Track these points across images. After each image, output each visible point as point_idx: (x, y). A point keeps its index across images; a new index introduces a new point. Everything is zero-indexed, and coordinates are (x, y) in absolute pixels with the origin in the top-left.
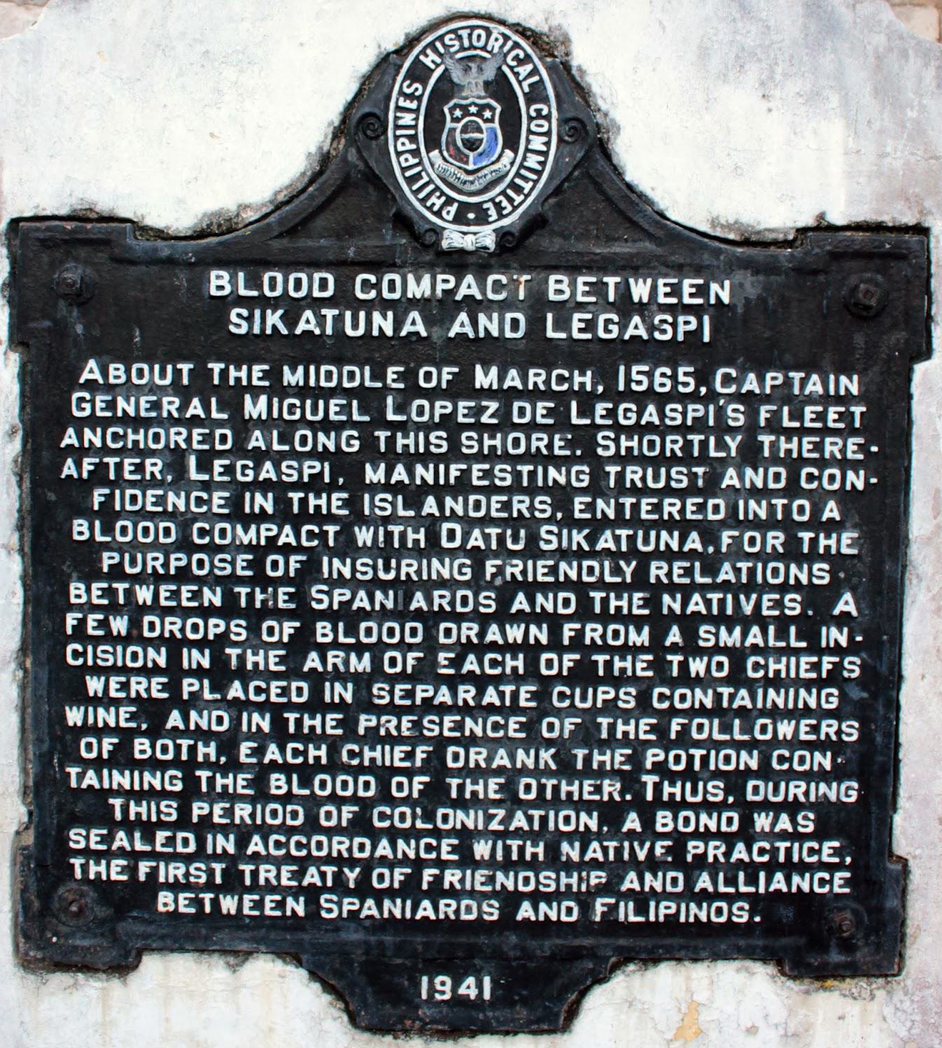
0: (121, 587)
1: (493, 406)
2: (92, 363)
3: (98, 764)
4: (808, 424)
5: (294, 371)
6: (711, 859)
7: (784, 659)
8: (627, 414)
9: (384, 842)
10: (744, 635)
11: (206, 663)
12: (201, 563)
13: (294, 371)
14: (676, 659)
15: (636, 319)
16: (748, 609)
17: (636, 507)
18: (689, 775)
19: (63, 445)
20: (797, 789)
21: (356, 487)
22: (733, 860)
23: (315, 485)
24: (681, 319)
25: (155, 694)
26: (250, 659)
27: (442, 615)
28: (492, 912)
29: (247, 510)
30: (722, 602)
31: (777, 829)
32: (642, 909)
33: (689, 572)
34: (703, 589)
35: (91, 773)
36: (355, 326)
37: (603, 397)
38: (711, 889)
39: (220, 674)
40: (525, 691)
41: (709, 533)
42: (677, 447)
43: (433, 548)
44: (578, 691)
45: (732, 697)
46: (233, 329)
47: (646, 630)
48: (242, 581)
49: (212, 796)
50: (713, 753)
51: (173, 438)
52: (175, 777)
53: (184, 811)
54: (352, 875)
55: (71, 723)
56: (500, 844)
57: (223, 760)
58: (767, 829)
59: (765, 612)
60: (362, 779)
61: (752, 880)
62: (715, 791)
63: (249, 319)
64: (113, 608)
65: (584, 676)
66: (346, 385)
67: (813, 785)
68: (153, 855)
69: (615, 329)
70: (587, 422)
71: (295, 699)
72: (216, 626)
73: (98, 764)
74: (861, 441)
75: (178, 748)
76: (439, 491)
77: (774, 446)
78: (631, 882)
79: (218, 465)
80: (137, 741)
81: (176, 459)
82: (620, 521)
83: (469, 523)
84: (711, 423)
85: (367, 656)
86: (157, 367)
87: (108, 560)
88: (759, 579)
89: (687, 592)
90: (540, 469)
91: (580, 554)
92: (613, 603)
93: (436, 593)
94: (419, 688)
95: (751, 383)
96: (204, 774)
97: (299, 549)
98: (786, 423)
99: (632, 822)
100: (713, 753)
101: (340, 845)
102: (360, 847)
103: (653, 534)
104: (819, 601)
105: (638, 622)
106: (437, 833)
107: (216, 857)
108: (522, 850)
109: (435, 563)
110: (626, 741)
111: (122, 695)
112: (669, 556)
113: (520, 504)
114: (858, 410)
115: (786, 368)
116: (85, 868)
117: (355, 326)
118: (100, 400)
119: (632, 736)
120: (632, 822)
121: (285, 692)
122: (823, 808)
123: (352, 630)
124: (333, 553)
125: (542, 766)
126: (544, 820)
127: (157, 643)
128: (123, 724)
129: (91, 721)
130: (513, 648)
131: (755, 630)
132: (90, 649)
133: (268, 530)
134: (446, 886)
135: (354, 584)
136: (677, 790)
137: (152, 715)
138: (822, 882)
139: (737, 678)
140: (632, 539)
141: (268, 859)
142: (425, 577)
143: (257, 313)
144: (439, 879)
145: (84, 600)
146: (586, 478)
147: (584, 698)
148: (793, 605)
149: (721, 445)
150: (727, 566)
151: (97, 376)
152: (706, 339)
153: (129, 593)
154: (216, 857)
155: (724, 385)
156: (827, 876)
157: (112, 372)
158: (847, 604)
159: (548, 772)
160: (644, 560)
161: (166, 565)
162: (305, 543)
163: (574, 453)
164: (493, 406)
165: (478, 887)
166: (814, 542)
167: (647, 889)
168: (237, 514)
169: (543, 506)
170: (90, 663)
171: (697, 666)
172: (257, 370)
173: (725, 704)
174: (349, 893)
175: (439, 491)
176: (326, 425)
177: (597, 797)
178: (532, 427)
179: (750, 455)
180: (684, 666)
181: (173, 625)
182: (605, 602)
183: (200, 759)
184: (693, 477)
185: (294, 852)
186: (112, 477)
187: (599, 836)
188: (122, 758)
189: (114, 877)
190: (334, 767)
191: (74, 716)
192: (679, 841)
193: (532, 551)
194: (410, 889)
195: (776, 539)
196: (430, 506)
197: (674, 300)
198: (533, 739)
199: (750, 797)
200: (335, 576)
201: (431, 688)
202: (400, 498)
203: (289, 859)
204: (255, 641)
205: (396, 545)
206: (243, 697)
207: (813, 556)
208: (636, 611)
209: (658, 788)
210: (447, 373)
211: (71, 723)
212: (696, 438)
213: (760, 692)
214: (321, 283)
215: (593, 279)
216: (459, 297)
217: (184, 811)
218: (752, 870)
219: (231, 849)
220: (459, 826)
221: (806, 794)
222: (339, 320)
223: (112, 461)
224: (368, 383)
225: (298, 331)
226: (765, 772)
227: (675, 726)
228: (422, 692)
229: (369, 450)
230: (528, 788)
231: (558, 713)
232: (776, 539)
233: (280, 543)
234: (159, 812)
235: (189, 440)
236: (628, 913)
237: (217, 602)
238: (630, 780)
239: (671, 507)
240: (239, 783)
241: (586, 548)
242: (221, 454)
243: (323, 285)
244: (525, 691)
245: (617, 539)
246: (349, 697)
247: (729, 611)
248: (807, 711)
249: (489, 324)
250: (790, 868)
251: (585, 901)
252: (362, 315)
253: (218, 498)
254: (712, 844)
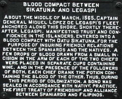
0: (11, 48)
1: (65, 22)
2: (6, 16)
3: (7, 74)
4: (110, 24)
5: (36, 17)
6: (96, 87)
7: (107, 58)
8: (84, 23)
9: (49, 85)
10: (101, 55)
11: (23, 59)
12: (22, 45)
13: (36, 17)
14: (91, 58)
15: (85, 9)
16: (101, 51)
17: (85, 36)
18: (93, 75)
19: (2, 28)
20: (109, 77)
21: (45, 33)
22: (100, 87)
23: (39, 33)
24: (92, 9)
25: (16, 64)
26: (30, 58)
27: (58, 52)
28: (65, 95)
29: (29, 37)
30: (98, 50)
31: (106, 83)
32: (86, 94)
33: (93, 45)
34: (95, 48)
35: (6, 76)
36: (45, 10)
37: (80, 20)
38: (96, 92)
39: (25, 61)
40: (70, 63)
41: (96, 40)
42: (91, 28)
43: (56, 42)
44: (77, 63)
45: (99, 63)
46: (27, 11)
47: (87, 54)
48: (29, 47)
49: (24, 79)
50: (96, 72)
51: (18, 27)
52: (19, 76)
53: (20, 81)
54: (45, 90)
55: (3, 68)
56: (66, 85)
57: (26, 73)
58: (105, 83)
59: (104, 51)
60: (46, 76)
61: (102, 90)
62: (97, 77)
63: (29, 9)
64: (10, 51)
65: (78, 60)
66: (44, 19)
67: (111, 76)
68: (15, 87)
69: (82, 11)
70: (78, 24)
71: (36, 64)
72: (25, 54)
73: (7, 74)
74: (118, 27)
75: (19, 72)
76: (57, 34)
77: (105, 27)
78: (85, 90)
79: (25, 30)
80: (13, 71)
81: (19, 30)
82: (83, 38)
83: (61, 39)
84: (96, 24)
85: (47, 58)
86: (16, 16)
87: (9, 44)
88: (103, 47)
89: (93, 48)
90: (71, 31)
91: (77, 43)
92: (82, 50)
93: (57, 49)
94: (54, 62)
95: (102, 18)
96: (23, 75)
97: (37, 42)
98: (107, 24)
99: (85, 82)
100: (96, 72)
101: (43, 85)
102: (45, 86)
103: (88, 40)
104: (112, 50)
105: (86, 53)
106: (57, 83)
107: (24, 87)
108: (69, 86)
109: (56, 44)
110: (84, 70)
111: (11, 64)
112: (90, 43)
113: (69, 36)
114: (117, 22)
115: (107, 16)
116: (5, 90)
117: (45, 10)
118: (8, 21)
119: (85, 69)
120: (85, 82)
121: (35, 63)
122: (113, 80)
123: (44, 54)
124: (42, 43)
125: (72, 74)
126: (72, 81)
127: (16, 56)
128: (11, 68)
129: (6, 68)
130: (68, 57)
131: (102, 54)
132: (6, 57)
133: (32, 40)
134: (58, 91)
135: (45, 47)
136: (91, 77)
137: (15, 67)
138: (113, 91)
139: (100, 61)
140: (85, 41)
141: (32, 87)
142: (55, 46)
143: (30, 8)
144: (57, 90)
145: (5, 50)
146: (78, 32)
147: (78, 64)
148: (108, 50)
149: (97, 27)
150: (98, 45)
151: (7, 18)
152: (95, 12)
153: (12, 49)
154: (24, 87)
155: (98, 19)
156: (113, 90)
157: (9, 17)
158: (116, 50)
159: (73, 74)
160: (86, 44)
161: (17, 45)
162: (38, 42)
163: (76, 28)
164: (65, 22)
165: (63, 91)
166: (111, 41)
167: (87, 91)
168: (28, 37)
169: (72, 36)
170: (6, 60)
171: (94, 59)
172: (31, 17)
173: (98, 65)
174: (44, 92)
175: (57, 34)
176: (41, 25)
177: (80, 78)
178: (70, 25)
179: (102, 29)
180: (92, 59)
181: (18, 54)
182: (81, 50)
183: (22, 73)
184: (93, 32)
185: (36, 87)
186: (9, 32)
187: (80, 84)
188: (11, 73)
189: (10, 91)
190: (42, 74)
191: (4, 67)
192: (92, 84)
193: (70, 43)
194: (53, 92)
195: (105, 41)
196: (56, 36)
197: (91, 7)
198: (71, 70)
199: (102, 78)
200: (42, 46)
201: (56, 62)
202: (51, 35)
203: (35, 87)
204: (30, 56)
205: (51, 42)
206: (29, 64)
207: (111, 43)
208: (85, 51)
209: (89, 77)
210: (58, 17)
211: (3, 68)
212: (94, 26)
213: (103, 63)
214: (40, 4)
215: (79, 4)
216: (60, 6)
217: (20, 81)
218: (102, 89)
219: (27, 86)
220: (60, 82)
221: (110, 78)
222: (42, 10)
223: (9, 30)
224: (47, 19)
225: (36, 11)
226: (104, 74)
227: (91, 68)
228: (55, 63)
229: (47, 28)
230: (70, 77)
231: (75, 66)
232: (105, 41)
233: (34, 42)
234: (16, 81)
235: (21, 27)
236: (84, 95)
237: (25, 50)
238: (85, 76)
239: (90, 36)
240: (28, 76)
241: (78, 42)
242: (25, 29)
243: (40, 4)
244: (70, 63)
245: (82, 41)
246: (44, 64)
247: (99, 51)
248: (110, 66)
249: (64, 10)
250: (108, 88)
251: (78, 93)
252: (46, 9)
253: (25, 35)
254: (96, 85)
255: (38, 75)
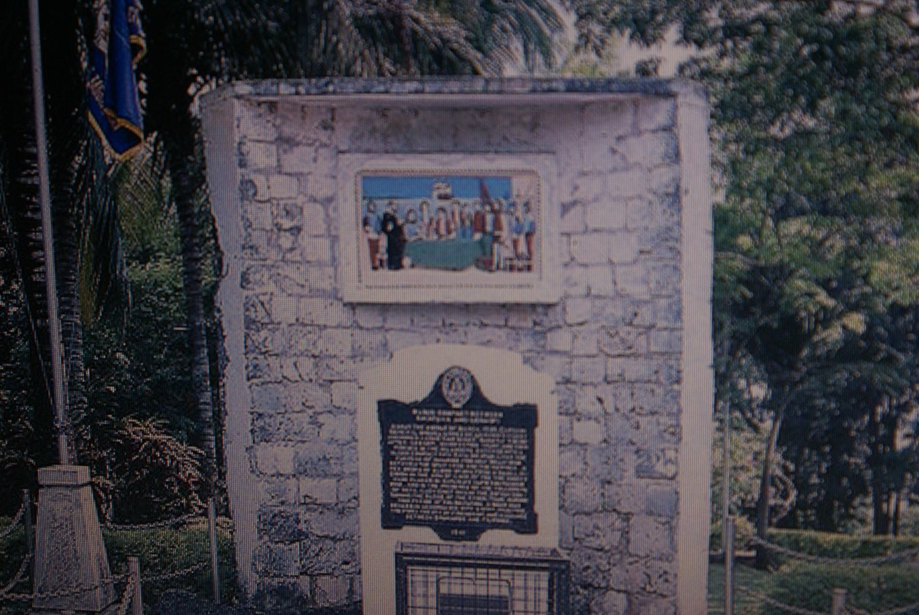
28: (464, 519)
39: (417, 477)
65: (479, 479)
148: (515, 468)
158: (524, 468)
188: (400, 492)
236: (488, 520)
255: (432, 494)
